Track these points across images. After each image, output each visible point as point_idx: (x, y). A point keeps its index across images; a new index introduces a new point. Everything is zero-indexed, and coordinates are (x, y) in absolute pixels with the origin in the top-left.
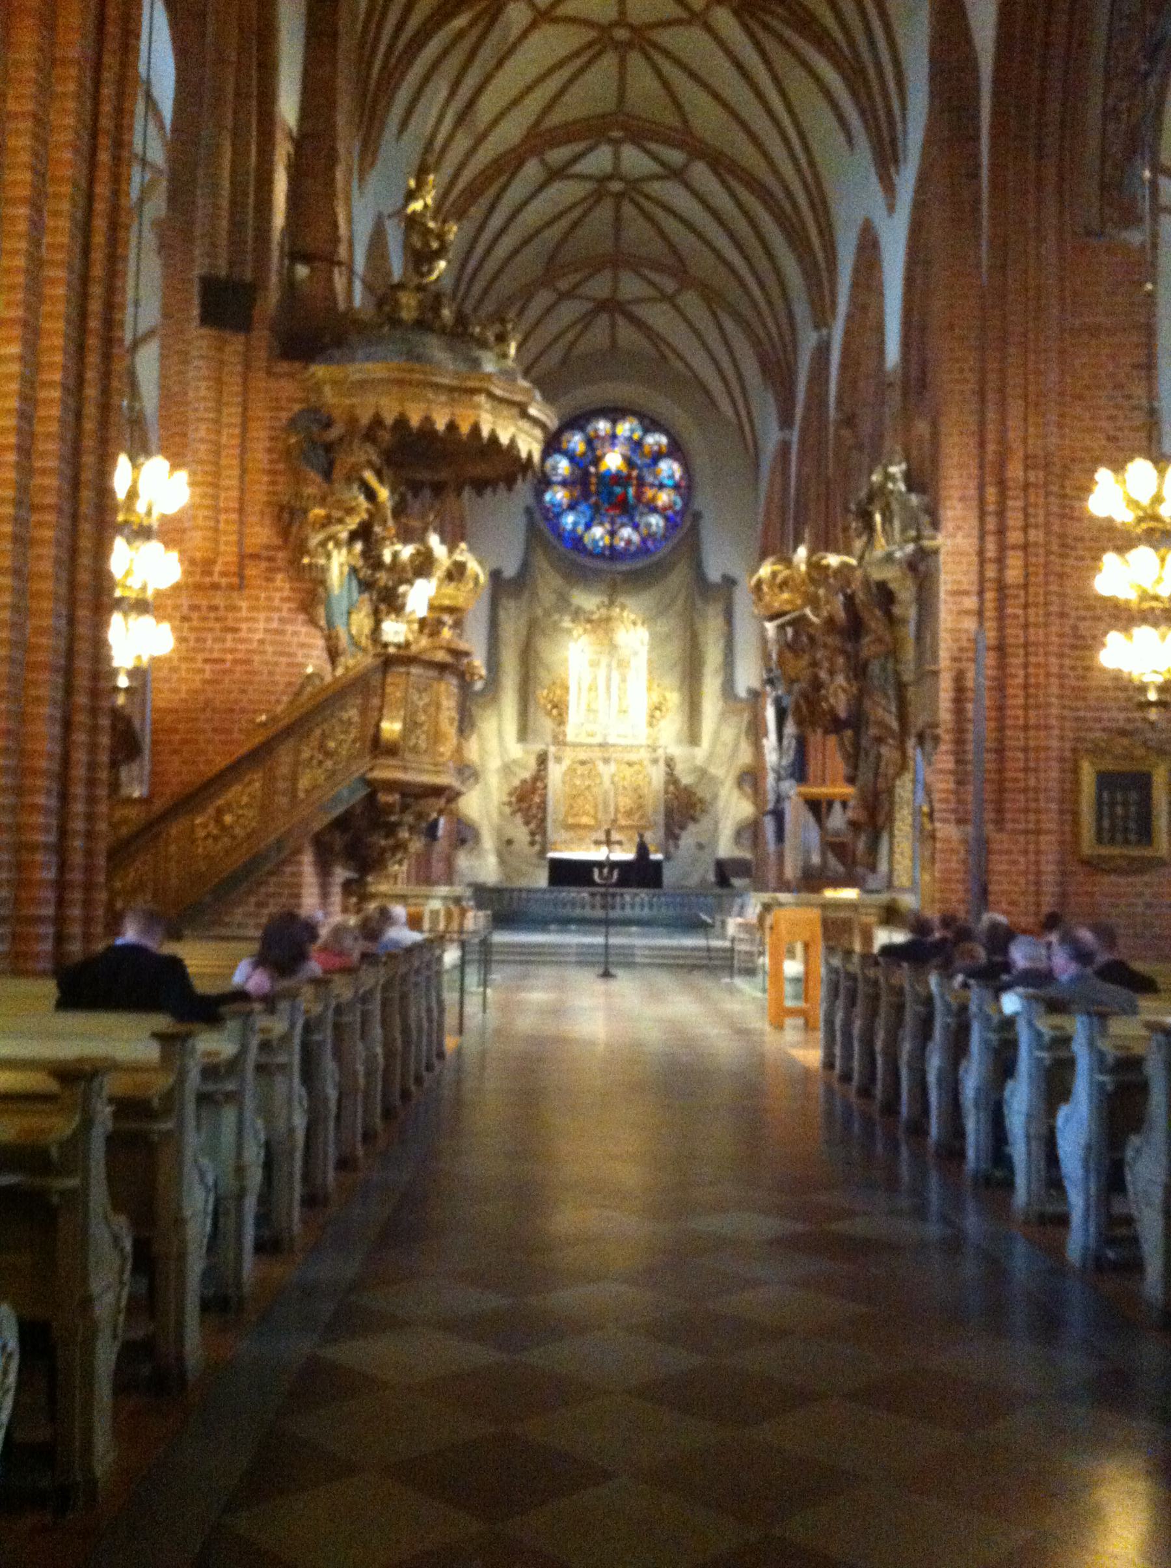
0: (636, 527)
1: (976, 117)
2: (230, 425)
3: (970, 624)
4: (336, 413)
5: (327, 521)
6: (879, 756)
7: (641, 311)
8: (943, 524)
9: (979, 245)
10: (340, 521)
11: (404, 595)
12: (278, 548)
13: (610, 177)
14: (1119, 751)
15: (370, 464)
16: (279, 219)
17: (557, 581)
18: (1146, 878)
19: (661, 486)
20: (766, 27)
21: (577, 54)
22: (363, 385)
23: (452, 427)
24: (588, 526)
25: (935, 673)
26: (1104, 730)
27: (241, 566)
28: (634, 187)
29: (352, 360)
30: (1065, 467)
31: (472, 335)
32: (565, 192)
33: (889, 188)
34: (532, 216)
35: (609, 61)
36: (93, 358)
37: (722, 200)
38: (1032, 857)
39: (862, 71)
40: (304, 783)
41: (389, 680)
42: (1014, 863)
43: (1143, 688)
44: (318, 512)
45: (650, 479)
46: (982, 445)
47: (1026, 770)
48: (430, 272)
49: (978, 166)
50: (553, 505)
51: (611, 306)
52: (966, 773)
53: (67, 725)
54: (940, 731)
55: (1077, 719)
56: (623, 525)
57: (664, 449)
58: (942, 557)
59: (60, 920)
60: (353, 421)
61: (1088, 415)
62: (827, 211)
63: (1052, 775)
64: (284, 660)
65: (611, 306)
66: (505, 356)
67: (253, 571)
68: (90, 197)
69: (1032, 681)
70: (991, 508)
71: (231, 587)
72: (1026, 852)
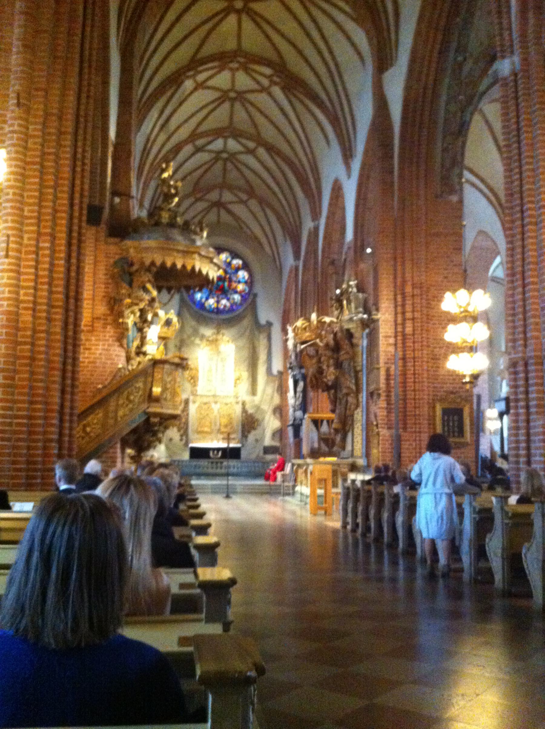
0: (228, 299)
3: (392, 349)
4: (135, 260)
5: (130, 306)
6: (347, 401)
8: (381, 309)
9: (393, 200)
10: (137, 304)
11: (146, 332)
12: (109, 315)
14: (450, 400)
15: (149, 281)
16: (109, 180)
17: (193, 323)
18: (463, 450)
19: (239, 282)
20: (295, 96)
21: (213, 102)
22: (147, 249)
23: (184, 266)
24: (207, 299)
25: (378, 369)
27: (93, 322)
28: (233, 156)
29: (142, 239)
32: (203, 157)
35: (227, 105)
36: (74, 248)
38: (418, 442)
40: (121, 413)
41: (156, 370)
42: (411, 445)
43: (464, 376)
44: (128, 301)
45: (234, 279)
48: (172, 202)
51: (219, 204)
52: (391, 409)
54: (381, 392)
55: (434, 387)
56: (223, 299)
57: (241, 266)
58: (380, 322)
60: (142, 263)
62: (318, 174)
63: (425, 410)
64: (109, 362)
65: (219, 204)
67: (98, 325)
68: (73, 185)
69: (417, 372)
70: (399, 303)
71: (88, 331)
72: (415, 440)
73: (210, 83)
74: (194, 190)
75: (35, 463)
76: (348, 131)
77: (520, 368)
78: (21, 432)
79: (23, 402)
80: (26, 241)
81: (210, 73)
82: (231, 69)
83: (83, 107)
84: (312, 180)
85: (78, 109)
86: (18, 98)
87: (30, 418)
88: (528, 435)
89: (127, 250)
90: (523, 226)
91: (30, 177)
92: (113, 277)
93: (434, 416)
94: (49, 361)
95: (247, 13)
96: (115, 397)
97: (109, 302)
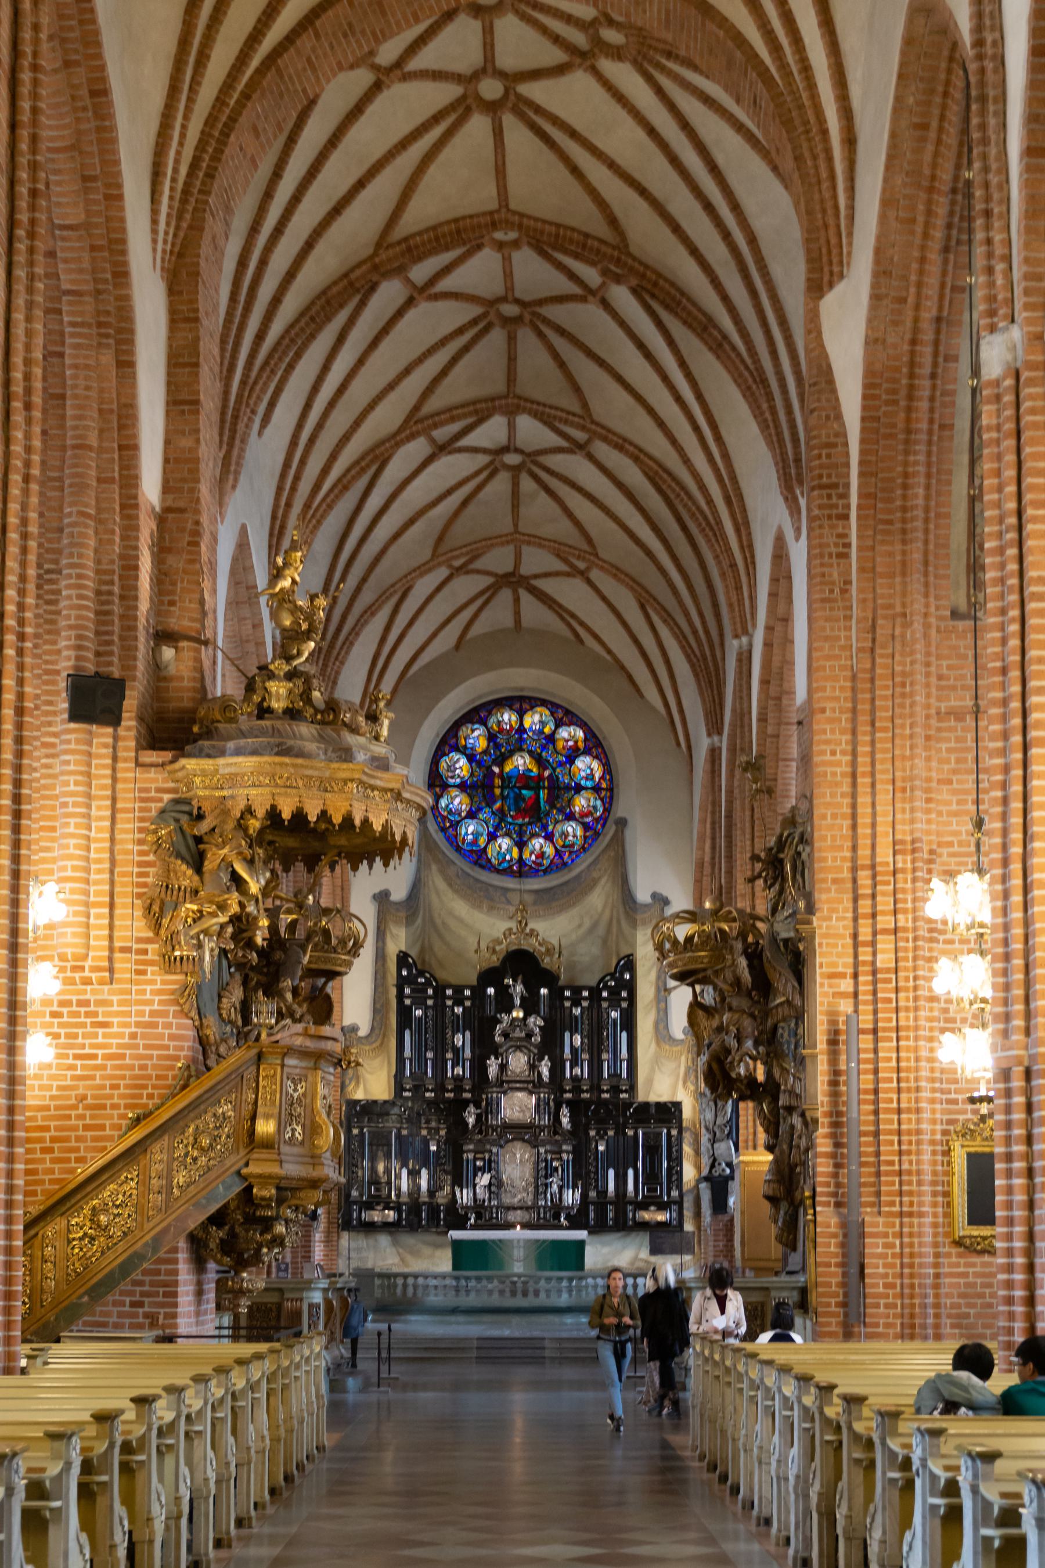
2: (100, 819)
4: (206, 807)
7: (546, 585)
10: (213, 915)
12: (148, 941)
13: (505, 449)
22: (233, 780)
23: (324, 815)
25: (814, 1057)
27: (110, 959)
28: (533, 459)
30: (932, 852)
31: (345, 724)
46: (854, 827)
49: (848, 545)
50: (450, 812)
60: (226, 813)
61: (955, 799)
66: (377, 738)
67: (124, 964)
74: (435, 554)
77: (1017, 1083)
96: (165, 1141)
97: (149, 908)
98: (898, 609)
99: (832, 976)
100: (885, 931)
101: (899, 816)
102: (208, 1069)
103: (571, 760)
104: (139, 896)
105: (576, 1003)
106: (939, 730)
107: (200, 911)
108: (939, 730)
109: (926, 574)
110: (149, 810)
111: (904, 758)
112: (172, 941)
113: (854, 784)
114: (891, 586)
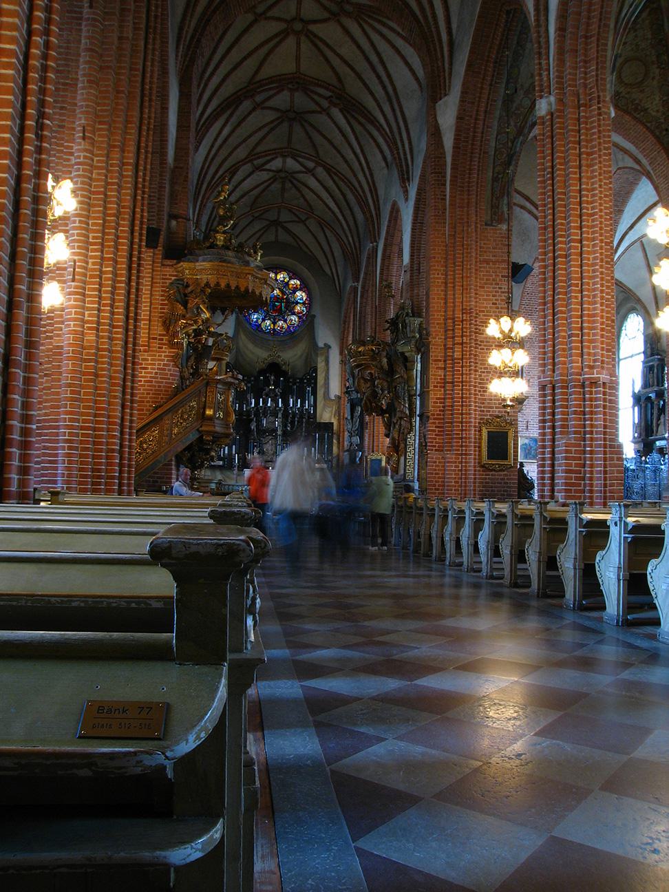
0: (285, 321)
1: (444, 177)
4: (190, 282)
10: (192, 325)
13: (280, 171)
15: (204, 303)
19: (297, 303)
20: (353, 116)
24: (264, 320)
25: (428, 392)
26: (490, 415)
27: (148, 342)
29: (197, 261)
30: (477, 314)
31: (246, 253)
33: (406, 192)
34: (247, 185)
35: (286, 124)
37: (330, 183)
39: (396, 144)
40: (176, 431)
41: (208, 390)
43: (504, 400)
47: (462, 430)
48: (227, 226)
51: (276, 223)
53: (123, 406)
56: (279, 320)
57: (299, 287)
59: (120, 478)
60: (198, 284)
65: (276, 223)
66: (256, 259)
68: (134, 213)
72: (462, 462)
73: (267, 104)
75: (99, 470)
76: (405, 154)
77: (548, 392)
78: (88, 442)
79: (88, 414)
80: (90, 266)
81: (272, 92)
82: (291, 90)
83: (143, 139)
84: (370, 201)
85: (139, 142)
86: (84, 132)
87: (95, 429)
88: (553, 453)
89: (183, 272)
90: (554, 258)
91: (95, 206)
92: (169, 298)
93: (480, 439)
94: (111, 378)
95: (307, 36)
97: (164, 323)
98: (466, 220)
99: (436, 361)
100: (458, 344)
101: (465, 299)
102: (183, 390)
103: (294, 292)
104: (161, 317)
105: (295, 384)
106: (480, 267)
107: (186, 323)
108: (480, 267)
109: (476, 208)
110: (166, 283)
111: (467, 277)
112: (175, 335)
113: (446, 287)
114: (463, 211)
